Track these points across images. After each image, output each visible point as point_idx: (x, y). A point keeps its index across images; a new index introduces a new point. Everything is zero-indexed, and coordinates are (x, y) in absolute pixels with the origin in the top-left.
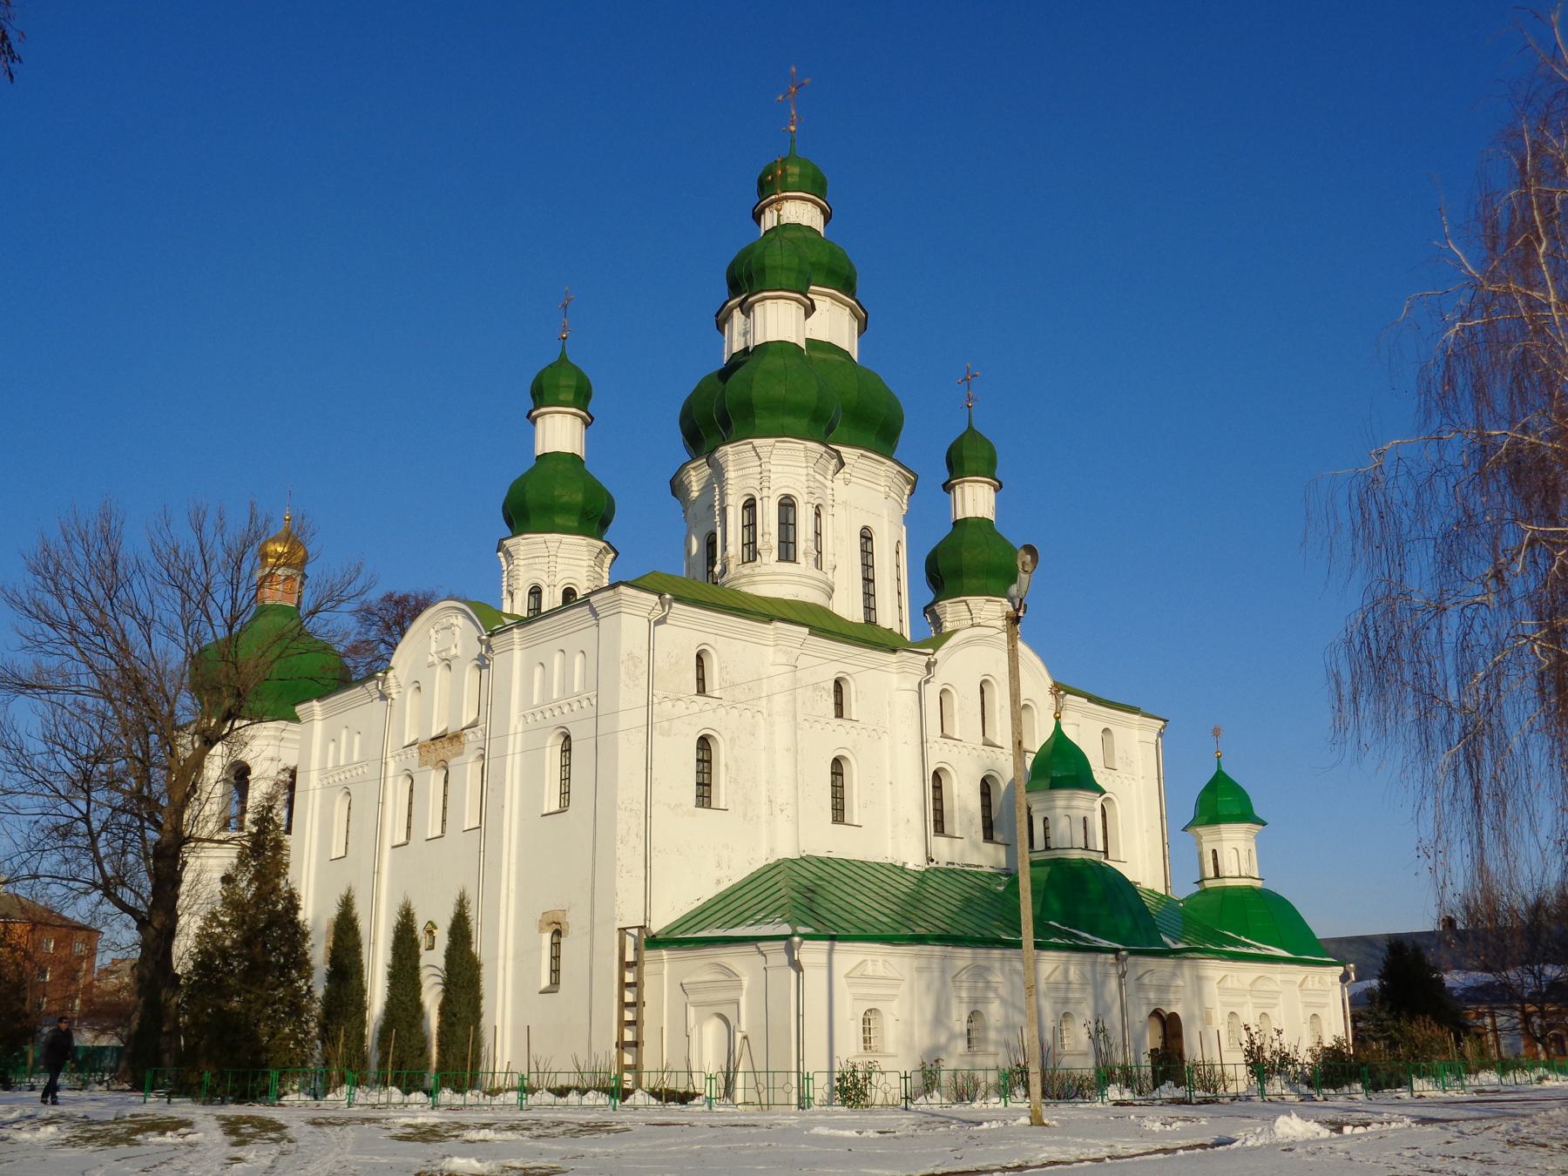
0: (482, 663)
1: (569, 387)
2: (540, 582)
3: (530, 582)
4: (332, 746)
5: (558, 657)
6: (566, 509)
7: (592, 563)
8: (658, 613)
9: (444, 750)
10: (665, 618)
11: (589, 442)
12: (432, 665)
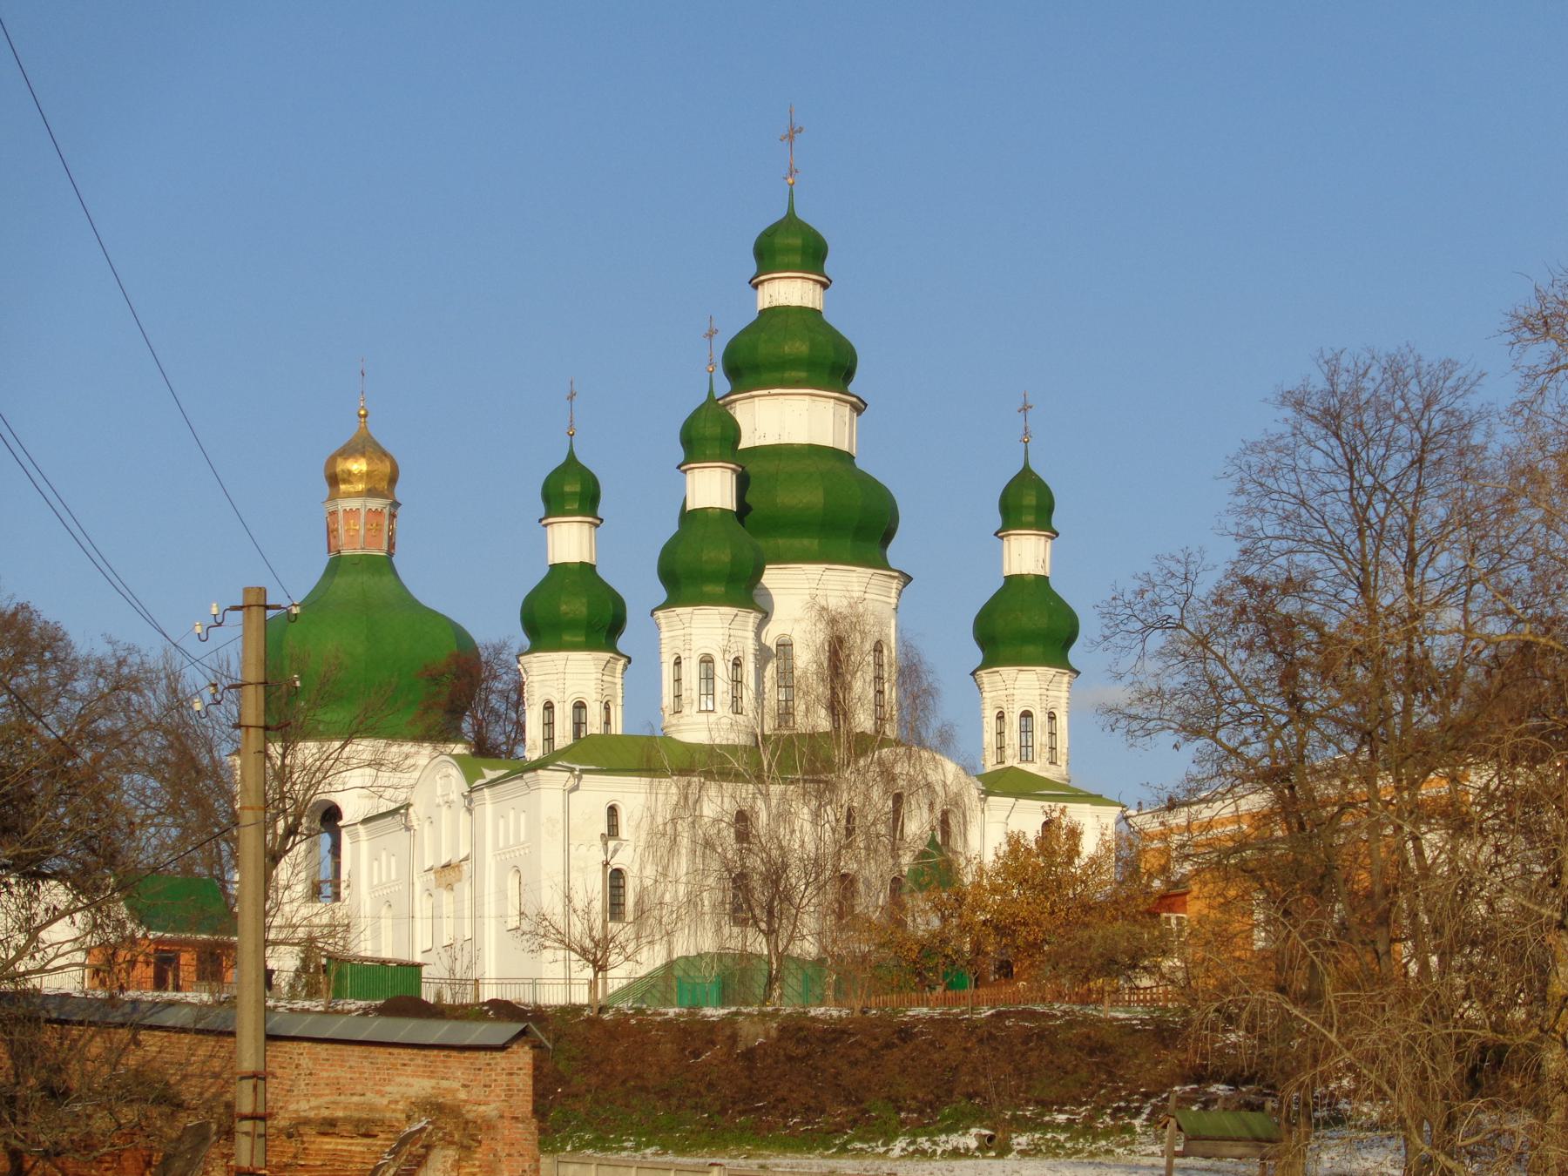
0: (470, 811)
1: (574, 494)
2: (553, 700)
3: (543, 698)
4: (376, 864)
5: (512, 814)
6: (572, 625)
7: (600, 676)
8: (572, 782)
9: (450, 875)
10: (578, 785)
11: (599, 545)
12: (439, 806)
